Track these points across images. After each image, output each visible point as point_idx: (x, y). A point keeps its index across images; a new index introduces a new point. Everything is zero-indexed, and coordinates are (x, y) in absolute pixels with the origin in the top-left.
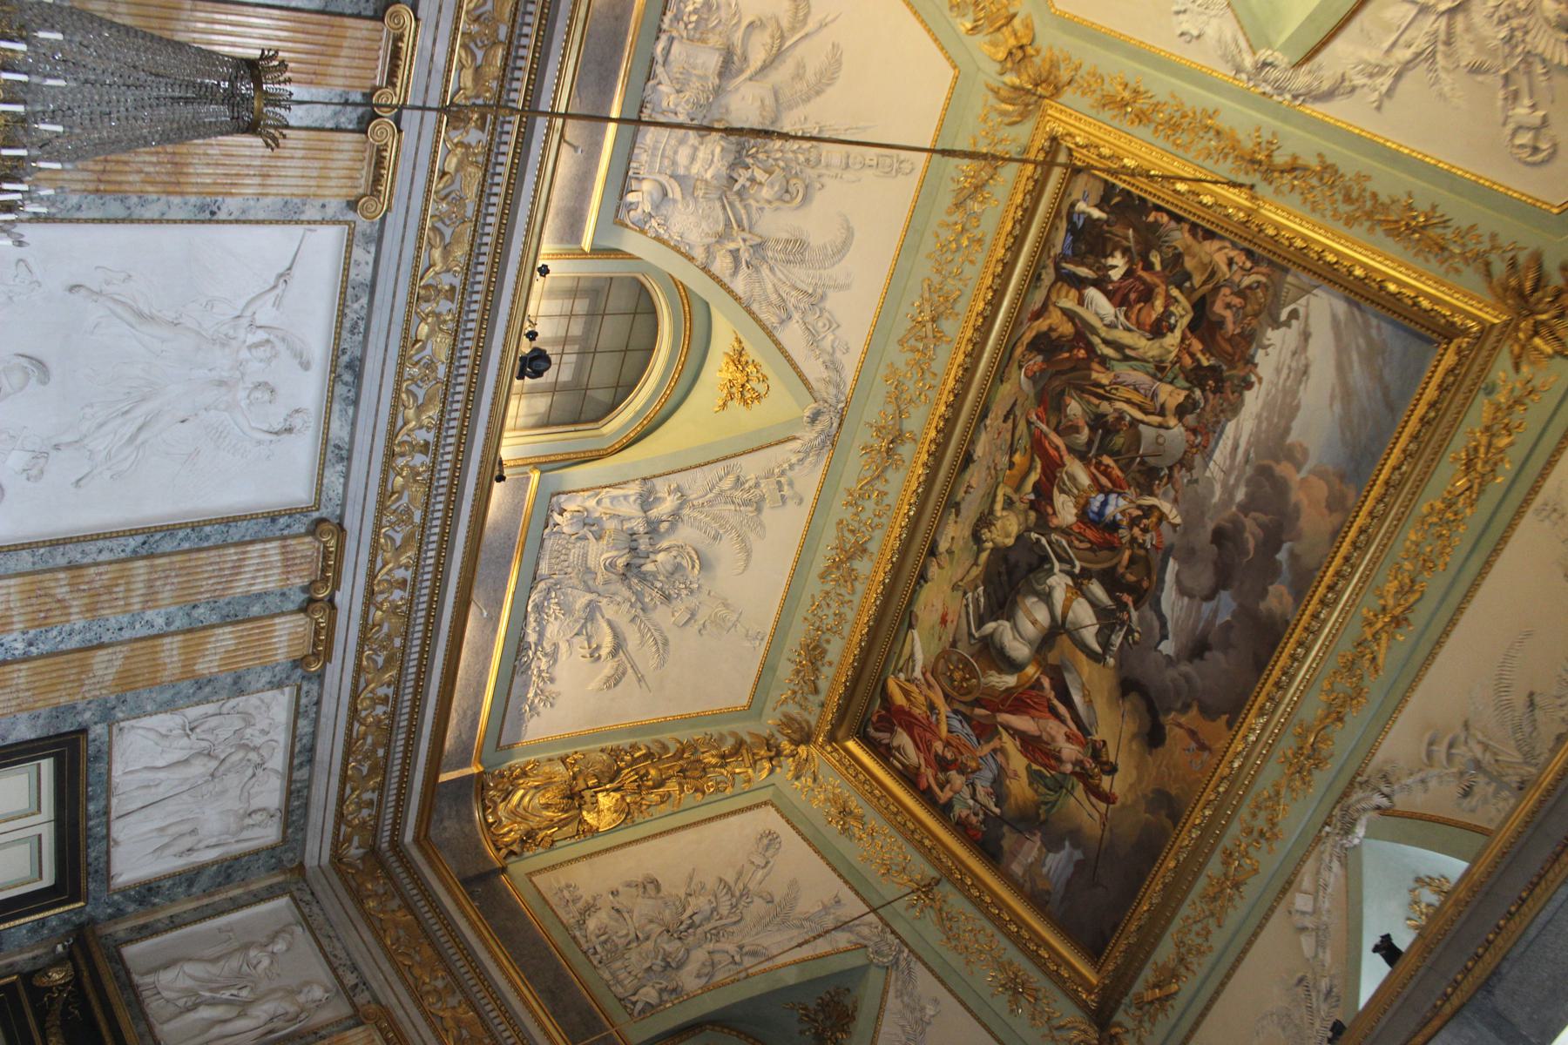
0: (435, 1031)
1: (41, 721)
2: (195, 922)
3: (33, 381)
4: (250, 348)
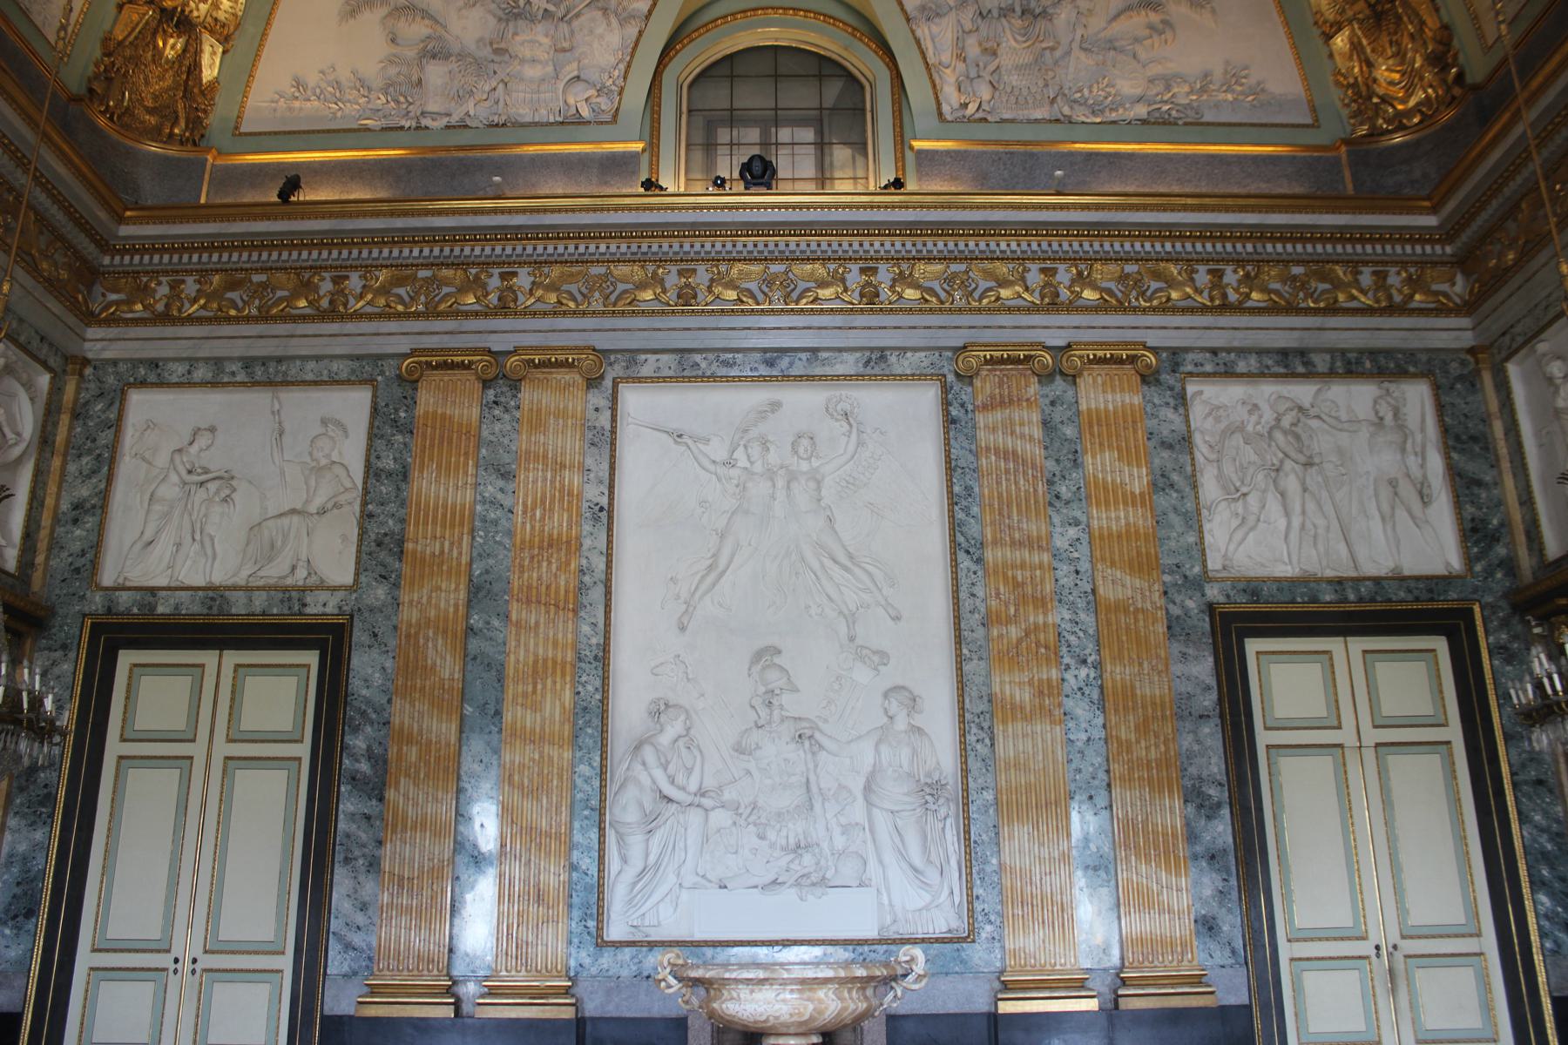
1: (1191, 651)
3: (777, 660)
4: (752, 463)
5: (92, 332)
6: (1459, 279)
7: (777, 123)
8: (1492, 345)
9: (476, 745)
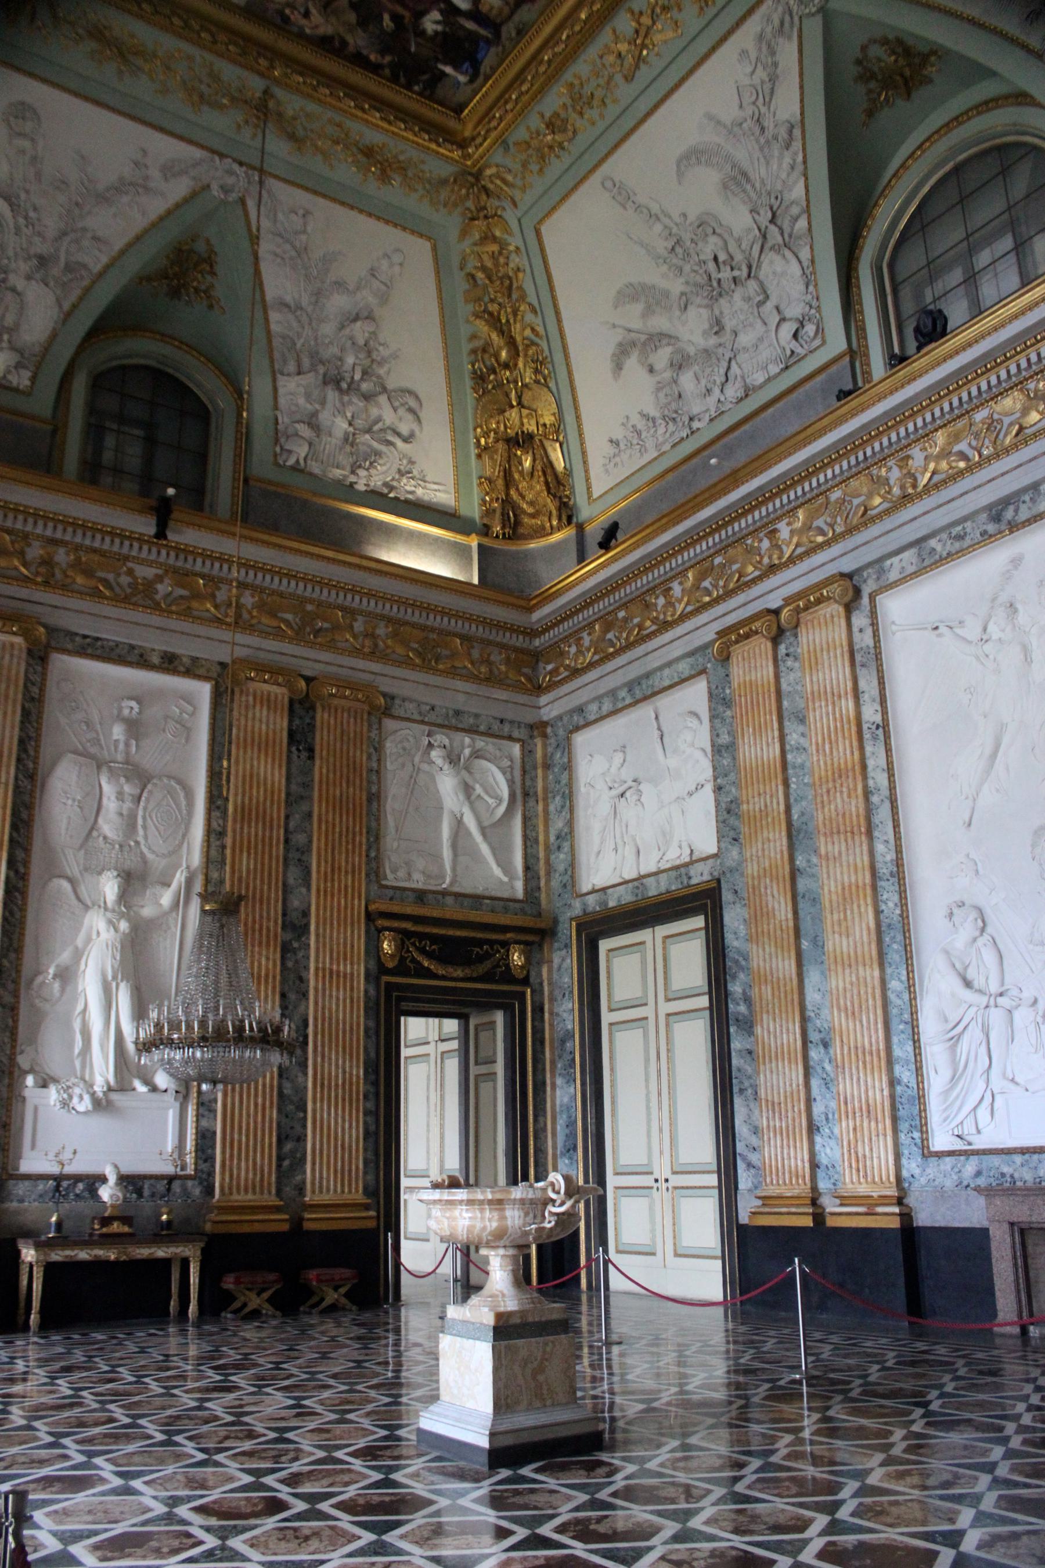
5: (544, 700)
7: (972, 252)
9: (813, 977)
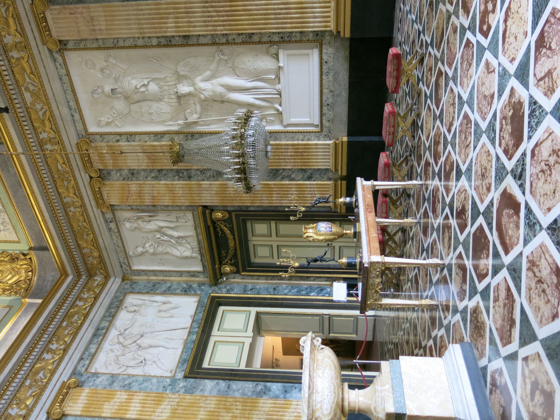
0: (79, 190)
1: (201, 388)
2: (172, 271)
6: (95, 278)
8: (124, 273)
